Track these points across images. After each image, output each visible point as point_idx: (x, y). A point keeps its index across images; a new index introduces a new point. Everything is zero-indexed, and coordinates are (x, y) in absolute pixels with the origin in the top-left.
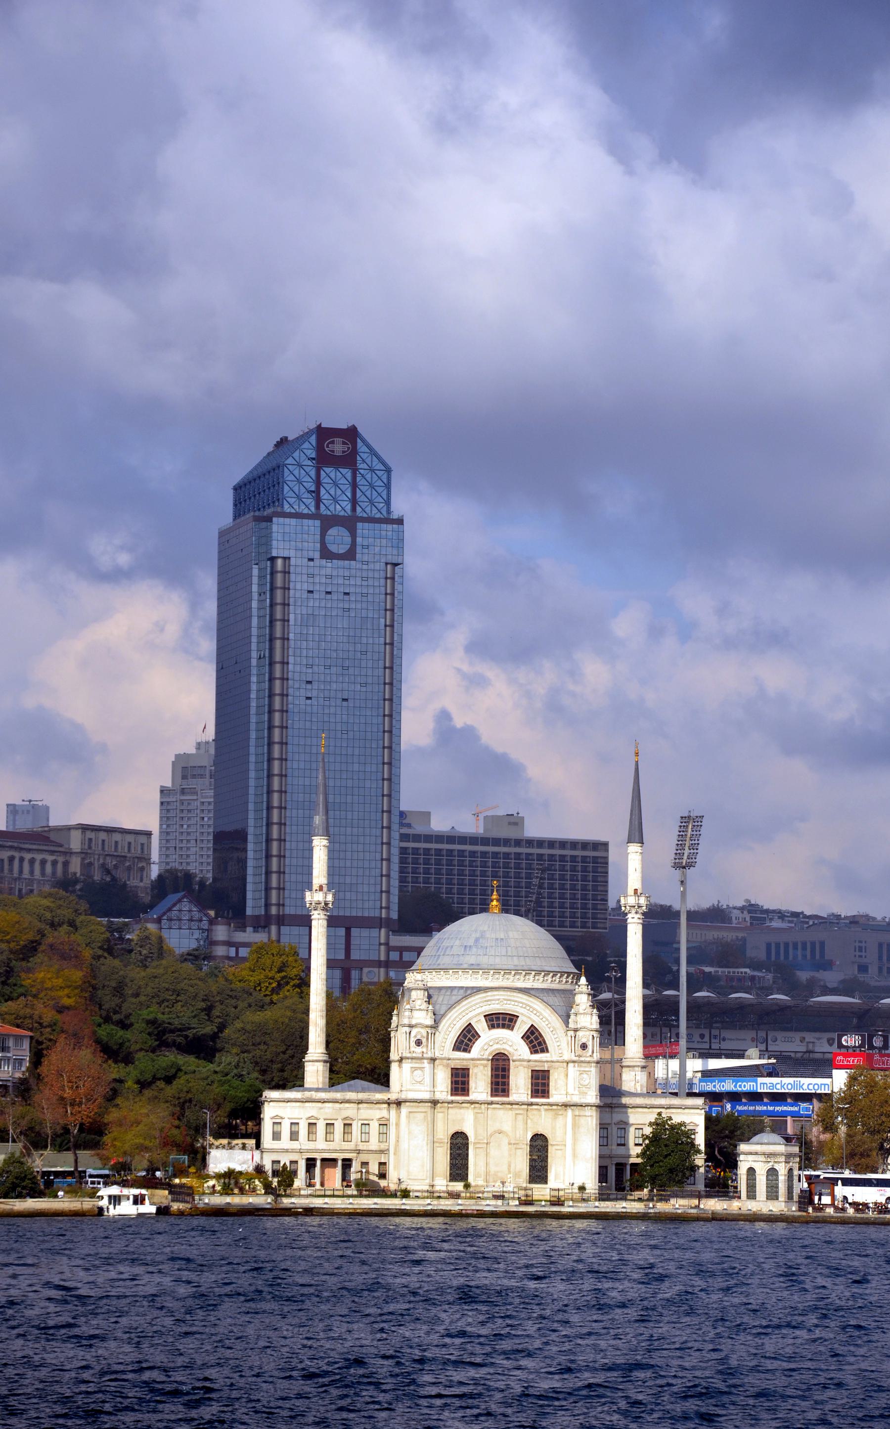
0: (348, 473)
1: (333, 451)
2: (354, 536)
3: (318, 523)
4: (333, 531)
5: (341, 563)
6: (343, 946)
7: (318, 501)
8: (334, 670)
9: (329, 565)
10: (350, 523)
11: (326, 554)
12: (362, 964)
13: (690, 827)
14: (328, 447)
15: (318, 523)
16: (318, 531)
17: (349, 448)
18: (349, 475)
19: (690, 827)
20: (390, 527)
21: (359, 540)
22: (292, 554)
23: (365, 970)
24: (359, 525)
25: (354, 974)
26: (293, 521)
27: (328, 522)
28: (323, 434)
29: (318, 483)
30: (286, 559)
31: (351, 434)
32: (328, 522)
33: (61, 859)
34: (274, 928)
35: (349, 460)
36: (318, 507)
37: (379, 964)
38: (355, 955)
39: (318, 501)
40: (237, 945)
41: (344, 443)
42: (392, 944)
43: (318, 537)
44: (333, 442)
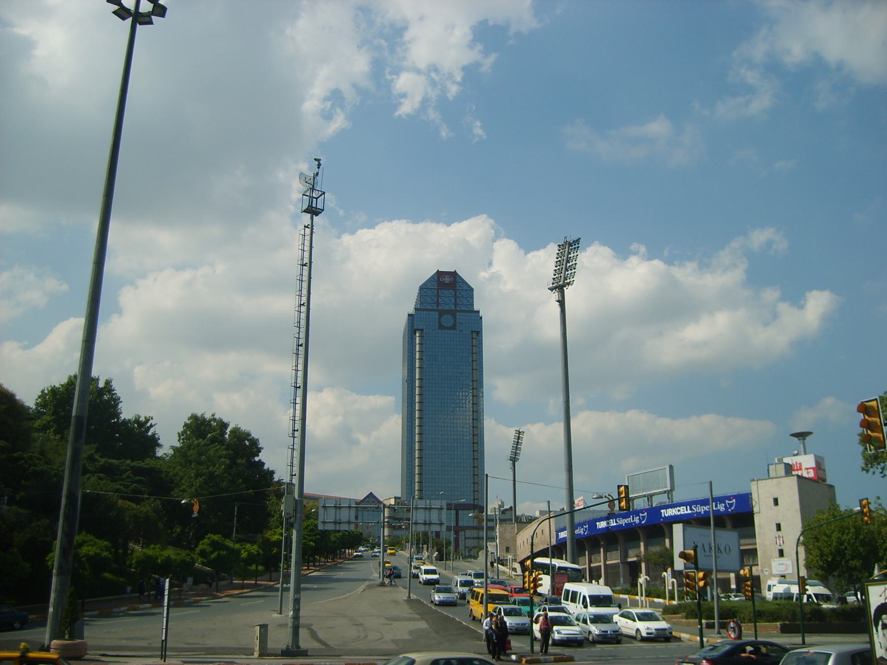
2: (455, 319)
5: (449, 331)
7: (438, 304)
11: (441, 327)
16: (437, 316)
18: (453, 293)
27: (442, 313)
29: (438, 296)
30: (422, 330)
31: (454, 274)
32: (442, 313)
38: (461, 524)
39: (438, 304)
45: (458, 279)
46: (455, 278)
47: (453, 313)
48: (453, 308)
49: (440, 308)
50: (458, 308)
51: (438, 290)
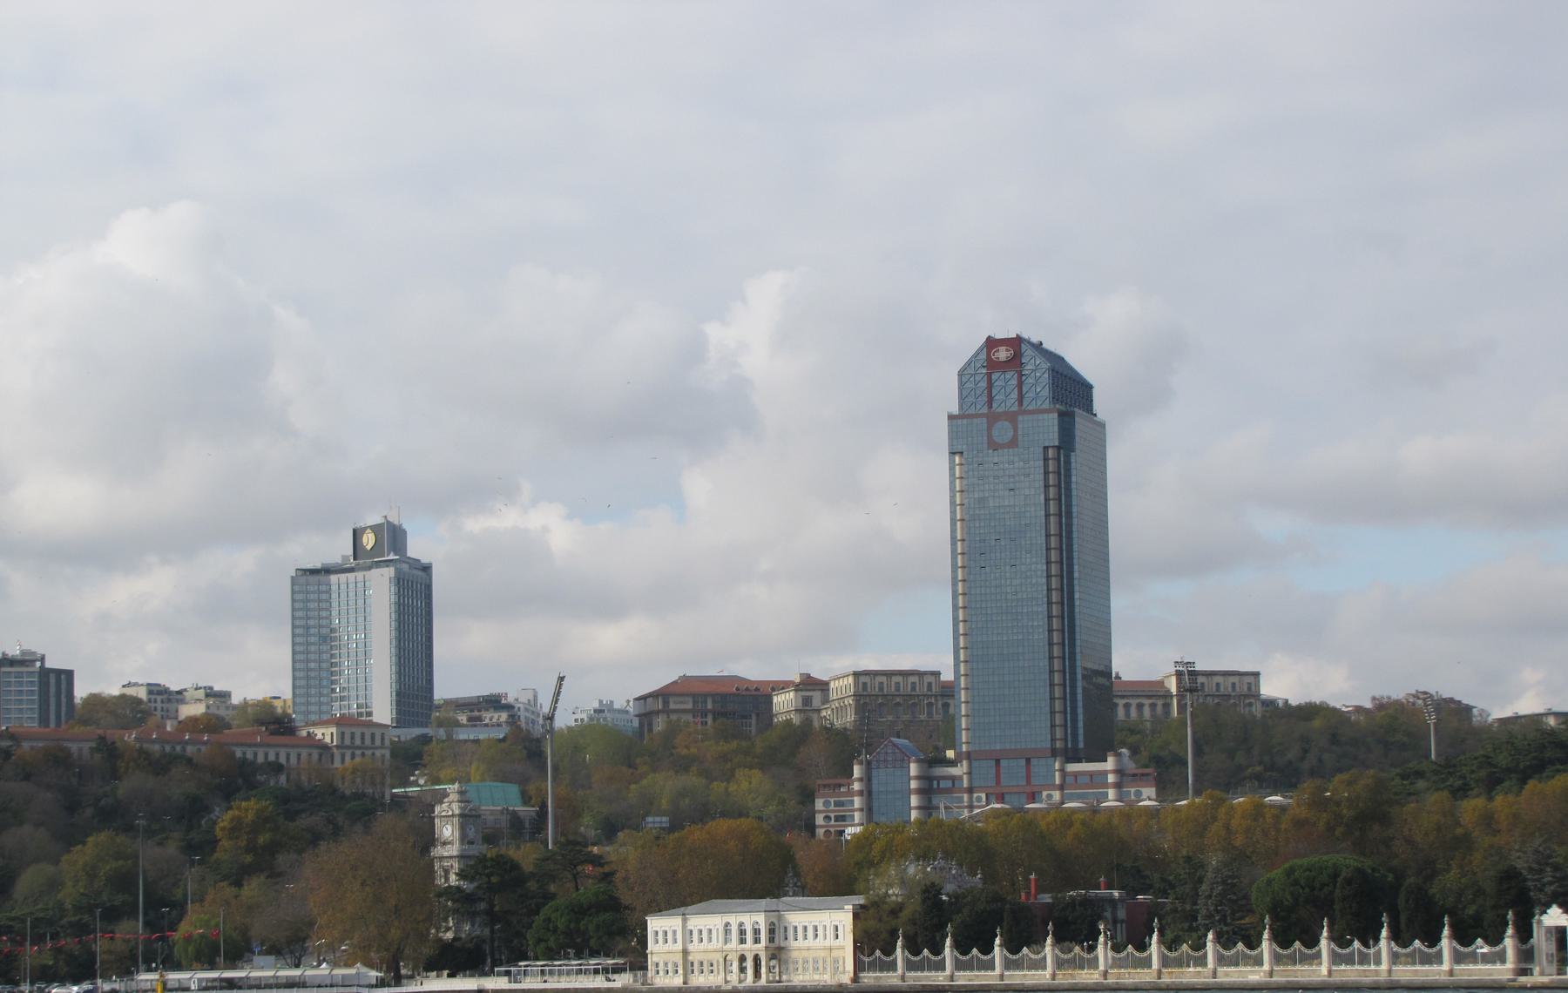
2: (1016, 430)
4: (998, 425)
11: (994, 446)
16: (985, 426)
23: (1045, 793)
27: (993, 418)
28: (991, 343)
31: (1016, 343)
33: (1160, 702)
38: (1034, 781)
47: (1012, 418)
51: (989, 375)
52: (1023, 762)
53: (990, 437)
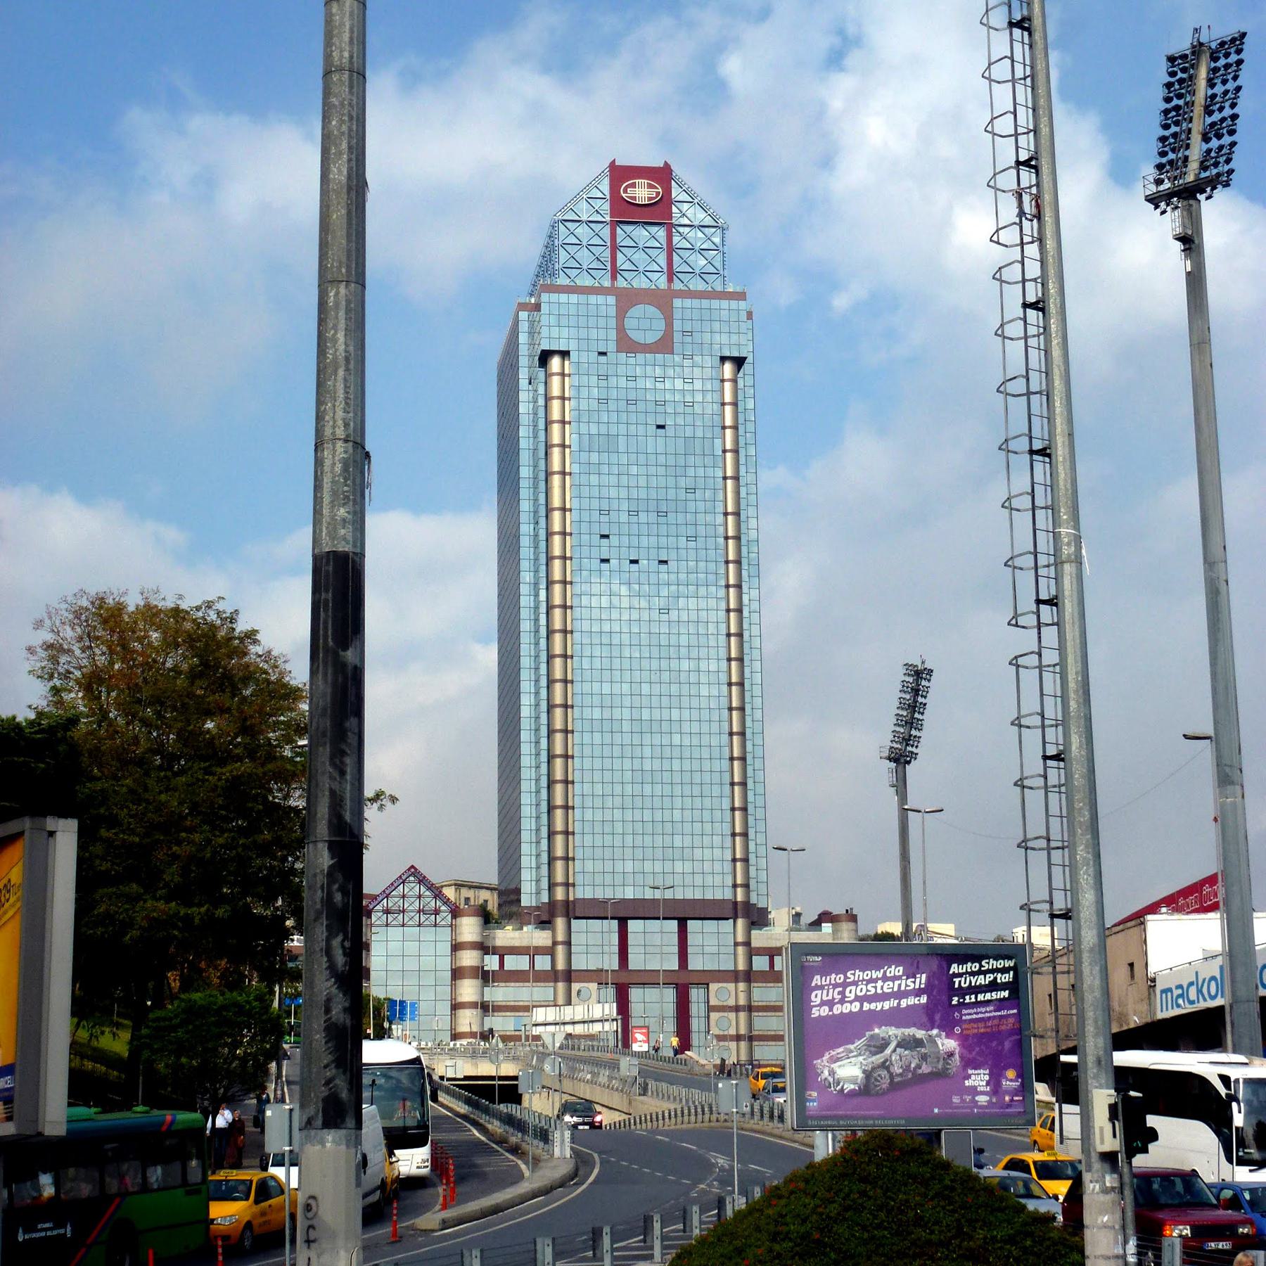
0: (661, 233)
1: (634, 198)
3: (611, 300)
4: (637, 311)
6: (676, 949)
8: (643, 517)
9: (632, 361)
10: (662, 301)
11: (626, 345)
12: (706, 979)
13: (1203, 73)
14: (625, 191)
15: (611, 300)
16: (612, 311)
17: (658, 193)
19: (1203, 73)
20: (725, 304)
21: (677, 325)
22: (572, 346)
23: (714, 987)
24: (677, 303)
25: (695, 994)
26: (574, 298)
27: (627, 300)
28: (620, 174)
30: (565, 354)
31: (663, 175)
32: (627, 300)
34: (560, 922)
35: (658, 212)
36: (614, 278)
37: (734, 976)
38: (695, 963)
39: (615, 272)
40: (502, 953)
41: (650, 186)
42: (755, 944)
43: (613, 323)
44: (633, 185)
45: (676, 192)
46: (668, 191)
47: (662, 301)
48: (662, 282)
49: (621, 283)
50: (677, 285)
51: (614, 225)
52: (674, 925)
53: (621, 330)
